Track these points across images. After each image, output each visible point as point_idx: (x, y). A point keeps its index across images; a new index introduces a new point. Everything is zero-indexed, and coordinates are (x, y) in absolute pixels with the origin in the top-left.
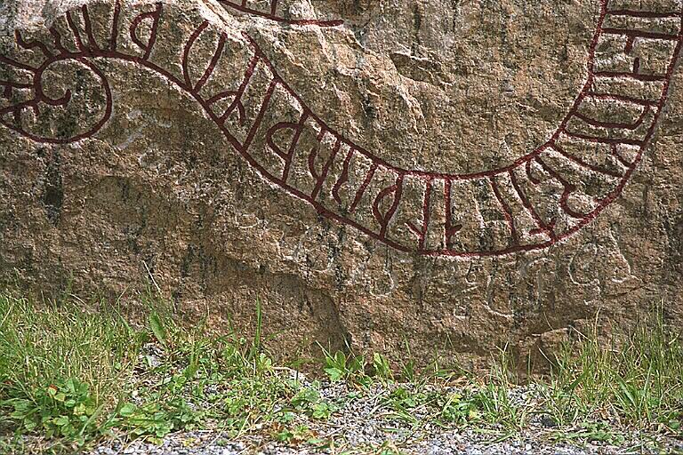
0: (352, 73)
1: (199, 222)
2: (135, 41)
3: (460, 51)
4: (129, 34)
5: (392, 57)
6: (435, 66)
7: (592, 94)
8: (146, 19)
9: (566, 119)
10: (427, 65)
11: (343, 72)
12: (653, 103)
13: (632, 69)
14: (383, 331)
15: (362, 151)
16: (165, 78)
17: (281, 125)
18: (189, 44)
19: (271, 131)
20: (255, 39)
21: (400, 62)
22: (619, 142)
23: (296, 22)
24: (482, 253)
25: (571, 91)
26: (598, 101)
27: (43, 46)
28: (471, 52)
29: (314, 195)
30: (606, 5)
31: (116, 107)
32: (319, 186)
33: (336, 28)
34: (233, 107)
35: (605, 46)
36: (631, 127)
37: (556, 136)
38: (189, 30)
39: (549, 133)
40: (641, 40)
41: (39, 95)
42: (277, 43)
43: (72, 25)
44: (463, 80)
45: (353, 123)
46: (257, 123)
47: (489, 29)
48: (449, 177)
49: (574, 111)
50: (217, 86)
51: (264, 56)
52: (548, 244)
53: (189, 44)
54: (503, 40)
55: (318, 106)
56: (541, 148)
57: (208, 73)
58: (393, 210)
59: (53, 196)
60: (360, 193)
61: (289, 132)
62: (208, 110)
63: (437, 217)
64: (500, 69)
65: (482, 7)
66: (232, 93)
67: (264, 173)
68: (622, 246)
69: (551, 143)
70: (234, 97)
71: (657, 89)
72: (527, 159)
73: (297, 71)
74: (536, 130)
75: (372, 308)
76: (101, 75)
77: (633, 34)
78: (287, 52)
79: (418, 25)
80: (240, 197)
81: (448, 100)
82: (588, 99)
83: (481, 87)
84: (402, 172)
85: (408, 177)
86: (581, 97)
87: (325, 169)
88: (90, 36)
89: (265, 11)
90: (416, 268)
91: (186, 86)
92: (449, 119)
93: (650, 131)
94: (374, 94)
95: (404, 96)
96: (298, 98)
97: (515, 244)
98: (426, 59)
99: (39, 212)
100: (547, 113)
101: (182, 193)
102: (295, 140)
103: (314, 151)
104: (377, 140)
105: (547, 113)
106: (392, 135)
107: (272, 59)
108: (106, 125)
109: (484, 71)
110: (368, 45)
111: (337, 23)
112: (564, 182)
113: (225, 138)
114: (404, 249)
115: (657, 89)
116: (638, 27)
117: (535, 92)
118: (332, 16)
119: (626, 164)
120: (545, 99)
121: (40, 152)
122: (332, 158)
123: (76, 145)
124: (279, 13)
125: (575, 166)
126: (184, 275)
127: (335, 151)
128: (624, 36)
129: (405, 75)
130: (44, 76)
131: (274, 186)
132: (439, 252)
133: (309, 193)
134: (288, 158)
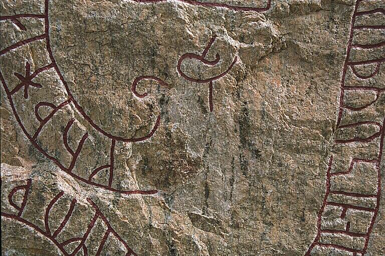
0: (162, 227)
2: (12, 204)
3: (234, 213)
4: (7, 200)
6: (218, 222)
7: (320, 244)
8: (20, 190)
10: (212, 221)
11: (156, 226)
12: (358, 251)
13: (345, 228)
16: (32, 229)
18: (50, 206)
20: (95, 203)
21: (195, 219)
23: (125, 192)
25: (307, 241)
26: (323, 248)
28: (242, 214)
30: (330, 187)
33: (152, 195)
34: (79, 248)
35: (327, 214)
38: (49, 197)
40: (351, 210)
42: (111, 206)
44: (236, 232)
47: (253, 199)
50: (68, 234)
51: (102, 214)
53: (50, 206)
54: (263, 207)
57: (62, 225)
62: (62, 250)
64: (261, 225)
65: (250, 185)
66: (79, 239)
70: (80, 241)
71: (360, 242)
77: (346, 207)
78: (118, 212)
81: (226, 244)
82: (318, 247)
83: (247, 237)
86: (313, 245)
89: (104, 184)
91: (47, 234)
94: (176, 240)
95: (196, 242)
96: (124, 243)
98: (212, 217)
107: (107, 216)
109: (250, 227)
110: (173, 207)
111: (153, 192)
115: (360, 242)
116: (349, 202)
117: (284, 243)
118: (150, 188)
120: (290, 246)
124: (114, 185)
128: (341, 208)
129: (197, 227)
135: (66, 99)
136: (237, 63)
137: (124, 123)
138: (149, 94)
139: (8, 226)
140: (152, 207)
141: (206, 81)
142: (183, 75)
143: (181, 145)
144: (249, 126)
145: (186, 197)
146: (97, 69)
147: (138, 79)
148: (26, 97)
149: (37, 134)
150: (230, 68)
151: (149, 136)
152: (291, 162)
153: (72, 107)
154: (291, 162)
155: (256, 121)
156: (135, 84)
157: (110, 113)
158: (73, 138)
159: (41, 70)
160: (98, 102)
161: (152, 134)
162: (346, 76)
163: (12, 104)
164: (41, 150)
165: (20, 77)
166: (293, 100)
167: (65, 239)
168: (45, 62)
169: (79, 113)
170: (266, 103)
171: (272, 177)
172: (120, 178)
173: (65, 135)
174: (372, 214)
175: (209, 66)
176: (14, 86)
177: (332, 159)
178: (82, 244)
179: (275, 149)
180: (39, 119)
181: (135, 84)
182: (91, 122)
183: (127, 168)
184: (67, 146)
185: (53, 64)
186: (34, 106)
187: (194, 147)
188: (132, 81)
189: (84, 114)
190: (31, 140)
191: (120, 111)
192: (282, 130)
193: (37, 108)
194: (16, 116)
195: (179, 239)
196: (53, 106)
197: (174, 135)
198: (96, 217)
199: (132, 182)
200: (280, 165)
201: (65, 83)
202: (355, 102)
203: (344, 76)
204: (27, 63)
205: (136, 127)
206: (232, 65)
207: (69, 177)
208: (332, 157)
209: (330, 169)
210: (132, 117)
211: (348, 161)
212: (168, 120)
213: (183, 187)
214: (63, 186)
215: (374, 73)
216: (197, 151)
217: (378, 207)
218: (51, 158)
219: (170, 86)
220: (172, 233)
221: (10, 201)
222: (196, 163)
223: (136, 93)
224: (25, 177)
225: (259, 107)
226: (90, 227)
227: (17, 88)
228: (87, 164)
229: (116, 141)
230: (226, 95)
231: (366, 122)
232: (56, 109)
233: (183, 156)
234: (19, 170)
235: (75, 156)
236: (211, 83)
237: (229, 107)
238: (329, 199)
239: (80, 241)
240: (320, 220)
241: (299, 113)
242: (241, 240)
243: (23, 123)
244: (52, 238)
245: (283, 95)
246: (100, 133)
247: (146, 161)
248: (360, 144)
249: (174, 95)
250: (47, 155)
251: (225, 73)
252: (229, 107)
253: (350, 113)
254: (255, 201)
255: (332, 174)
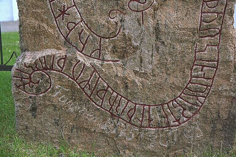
0: (122, 76)
1: (76, 118)
2: (59, 66)
3: (153, 70)
4: (57, 64)
5: (133, 71)
7: (191, 83)
9: (184, 90)
10: (144, 73)
12: (209, 86)
14: (129, 149)
15: (125, 98)
17: (101, 90)
18: (74, 67)
19: (98, 92)
20: (93, 66)
21: (136, 73)
22: (199, 96)
23: (106, 61)
24: (159, 127)
25: (186, 82)
27: (32, 67)
28: (157, 70)
29: (110, 110)
31: (53, 85)
32: (111, 108)
33: (118, 62)
34: (87, 85)
35: (195, 70)
36: (202, 92)
37: (181, 94)
38: (74, 63)
39: (179, 93)
40: (205, 68)
41: (31, 81)
42: (100, 67)
43: (40, 61)
44: (154, 78)
45: (122, 90)
46: (94, 90)
47: (162, 64)
48: (149, 106)
49: (186, 87)
50: (82, 79)
52: (178, 125)
53: (74, 67)
55: (111, 85)
56: (177, 98)
57: (80, 75)
58: (133, 115)
59: (34, 109)
60: (123, 110)
61: (103, 92)
62: (80, 86)
63: (146, 117)
65: (160, 57)
66: (87, 81)
67: (96, 104)
68: (200, 127)
69: (179, 96)
70: (87, 82)
71: (209, 82)
72: (172, 101)
73: (106, 75)
74: (175, 93)
75: (126, 143)
76: (48, 76)
77: (203, 66)
78: (103, 69)
79: (141, 62)
80: (88, 110)
82: (190, 84)
83: (158, 80)
84: (136, 104)
85: (137, 105)
86: (188, 84)
87: (113, 103)
88: (46, 64)
89: (96, 58)
90: (140, 131)
91: (73, 79)
92: (150, 89)
93: (208, 94)
95: (137, 82)
97: (168, 125)
98: (144, 72)
99: (30, 114)
100: (179, 88)
101: (71, 110)
102: (105, 95)
103: (110, 97)
104: (129, 94)
105: (179, 88)
106: (133, 94)
108: (50, 90)
109: (160, 76)
110: (127, 67)
111: (118, 61)
112: (183, 108)
113: (84, 94)
114: (136, 126)
115: (209, 82)
116: (205, 64)
119: (201, 103)
121: (30, 97)
122: (116, 100)
123: (41, 95)
125: (186, 103)
126: (72, 132)
127: (116, 98)
129: (137, 76)
130: (32, 76)
131: (98, 107)
132: (146, 127)
133: (109, 110)
134: (103, 99)
135: (80, 20)
136: (154, 3)
137: (105, 30)
138: (116, 18)
139: (57, 75)
140: (117, 68)
141: (141, 11)
142: (130, 9)
143: (130, 40)
144: (159, 31)
145: (132, 64)
146: (93, 7)
147: (111, 11)
148: (63, 19)
149: (67, 36)
150: (151, 6)
151: (115, 36)
152: (178, 47)
153: (83, 24)
154: (178, 47)
155: (162, 28)
156: (109, 13)
157: (99, 26)
158: (83, 37)
159: (70, 8)
160: (94, 22)
161: (117, 35)
162: (203, 8)
163: (57, 23)
164: (69, 42)
165: (60, 11)
166: (179, 19)
167: (81, 81)
168: (71, 4)
169: (86, 26)
170: (167, 21)
171: (170, 54)
172: (104, 55)
173: (80, 36)
174: (215, 69)
175: (142, 5)
176: (58, 15)
177: (197, 45)
178: (88, 83)
179: (171, 41)
180: (69, 29)
181: (109, 13)
182: (91, 30)
183: (107, 51)
184: (80, 41)
185: (75, 5)
186: (67, 23)
187: (135, 40)
188: (108, 12)
189: (88, 27)
190: (65, 39)
191: (104, 25)
192: (174, 33)
193: (68, 24)
194: (58, 28)
195: (129, 81)
196: (75, 23)
197: (127, 35)
198: (94, 71)
199: (108, 57)
200: (173, 48)
201: (80, 13)
202: (207, 19)
203: (202, 7)
204: (64, 5)
205: (110, 32)
206: (152, 4)
207: (82, 54)
208: (197, 44)
209: (196, 49)
210: (108, 28)
211: (204, 46)
212: (124, 29)
213: (131, 59)
214: (79, 58)
215: (216, 6)
216: (137, 42)
217: (217, 66)
218: (74, 46)
219: (125, 14)
220: (126, 78)
221: (58, 64)
222: (136, 48)
223: (110, 17)
224: (64, 54)
225: (164, 23)
226: (91, 76)
227: (59, 16)
228: (89, 49)
229: (102, 39)
230: (149, 18)
231: (213, 28)
232: (76, 25)
233: (131, 45)
234: (61, 52)
235: (84, 45)
236: (143, 12)
237: (151, 22)
238: (196, 63)
239: (87, 82)
240: (191, 72)
241: (181, 24)
242: (156, 81)
243: (61, 31)
244: (75, 81)
245: (175, 16)
246: (95, 35)
247: (114, 47)
248: (210, 38)
249: (127, 18)
250: (72, 45)
251: (149, 8)
252: (151, 23)
253: (205, 24)
254: (162, 64)
255: (197, 52)
